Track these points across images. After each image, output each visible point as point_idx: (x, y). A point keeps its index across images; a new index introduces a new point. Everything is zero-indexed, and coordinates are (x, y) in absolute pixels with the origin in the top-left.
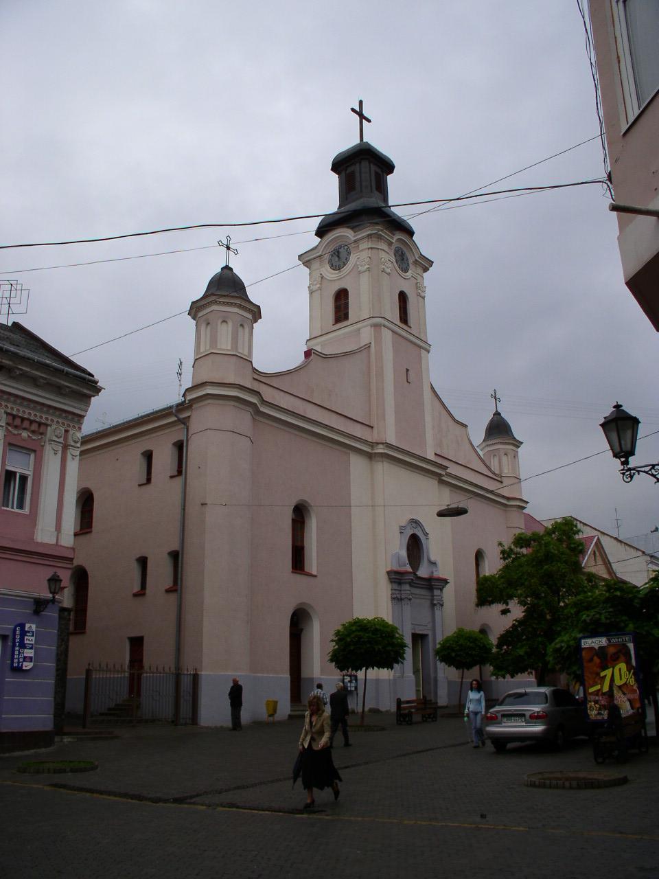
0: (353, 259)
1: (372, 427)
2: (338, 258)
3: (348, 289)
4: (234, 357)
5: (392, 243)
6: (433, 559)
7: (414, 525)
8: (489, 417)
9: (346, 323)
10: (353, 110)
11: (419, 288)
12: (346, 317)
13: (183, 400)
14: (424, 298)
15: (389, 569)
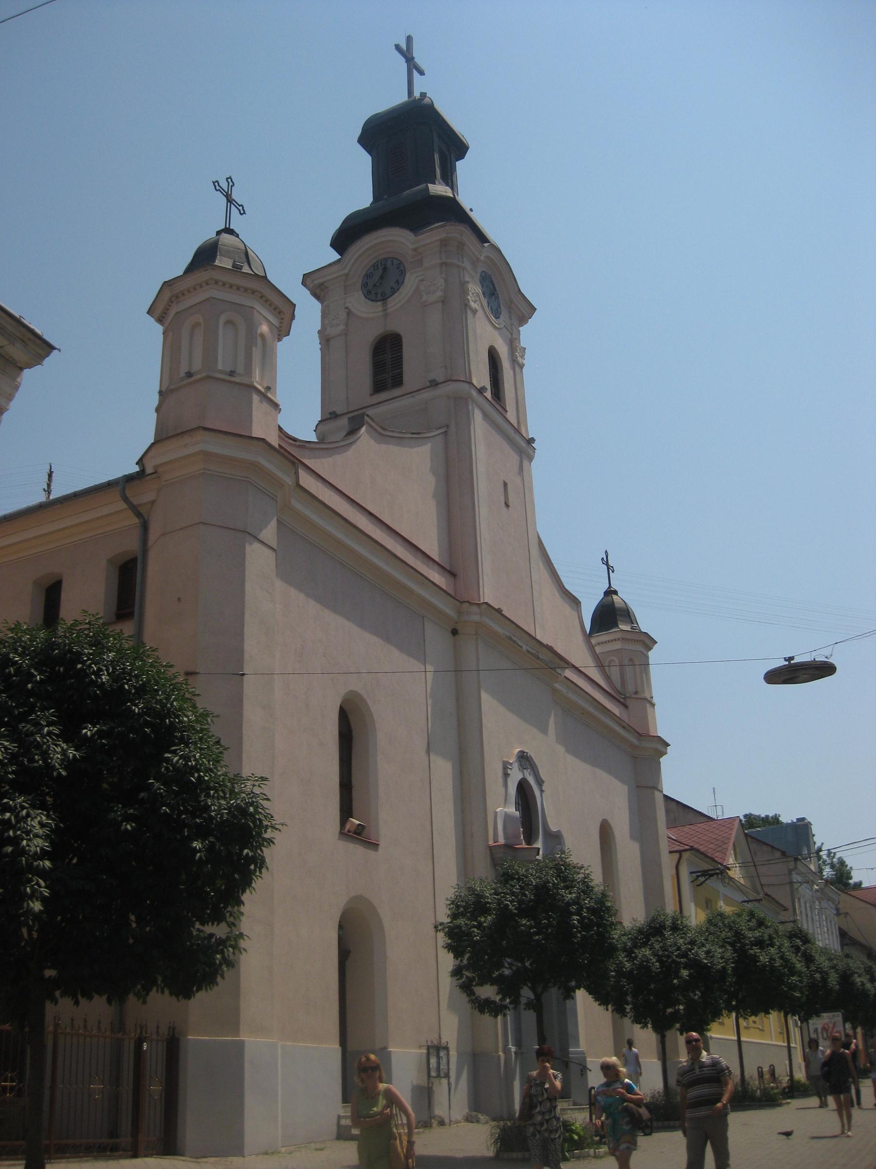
0: (411, 281)
2: (381, 281)
3: (402, 333)
5: (478, 259)
6: (553, 828)
9: (397, 392)
10: (398, 47)
11: (513, 344)
12: (398, 381)
13: (137, 469)
14: (521, 366)
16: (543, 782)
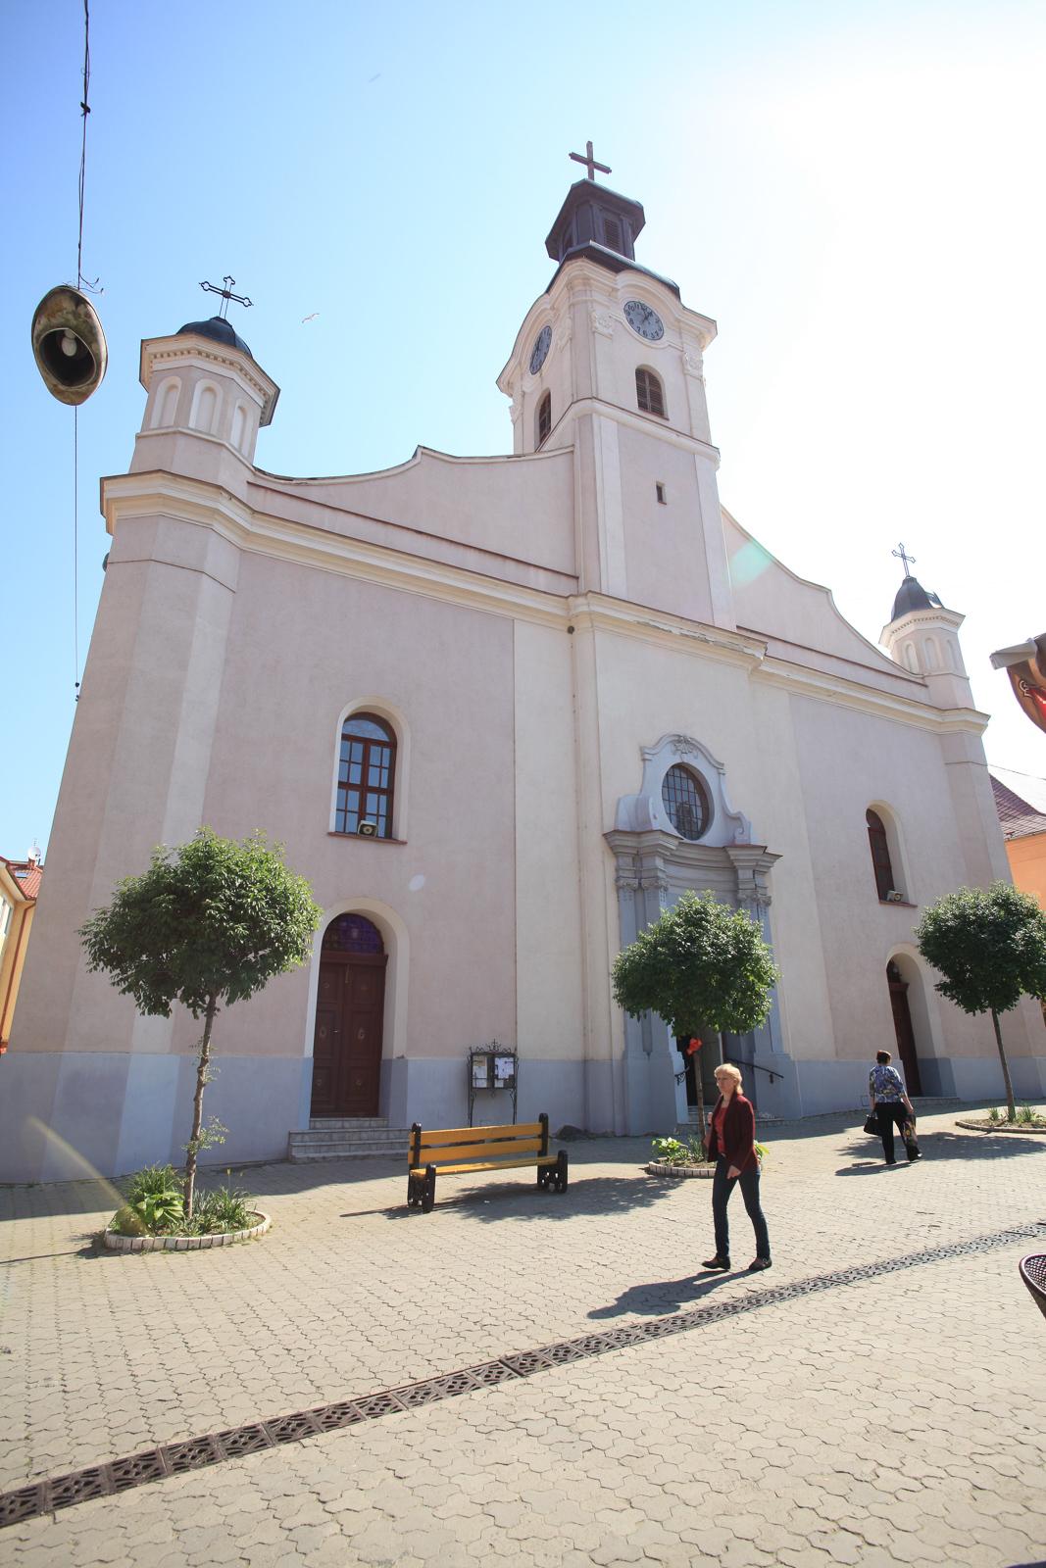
1: (577, 578)
4: (178, 435)
5: (615, 290)
6: (733, 810)
7: (682, 746)
8: (895, 586)
15: (609, 827)
16: (723, 764)
